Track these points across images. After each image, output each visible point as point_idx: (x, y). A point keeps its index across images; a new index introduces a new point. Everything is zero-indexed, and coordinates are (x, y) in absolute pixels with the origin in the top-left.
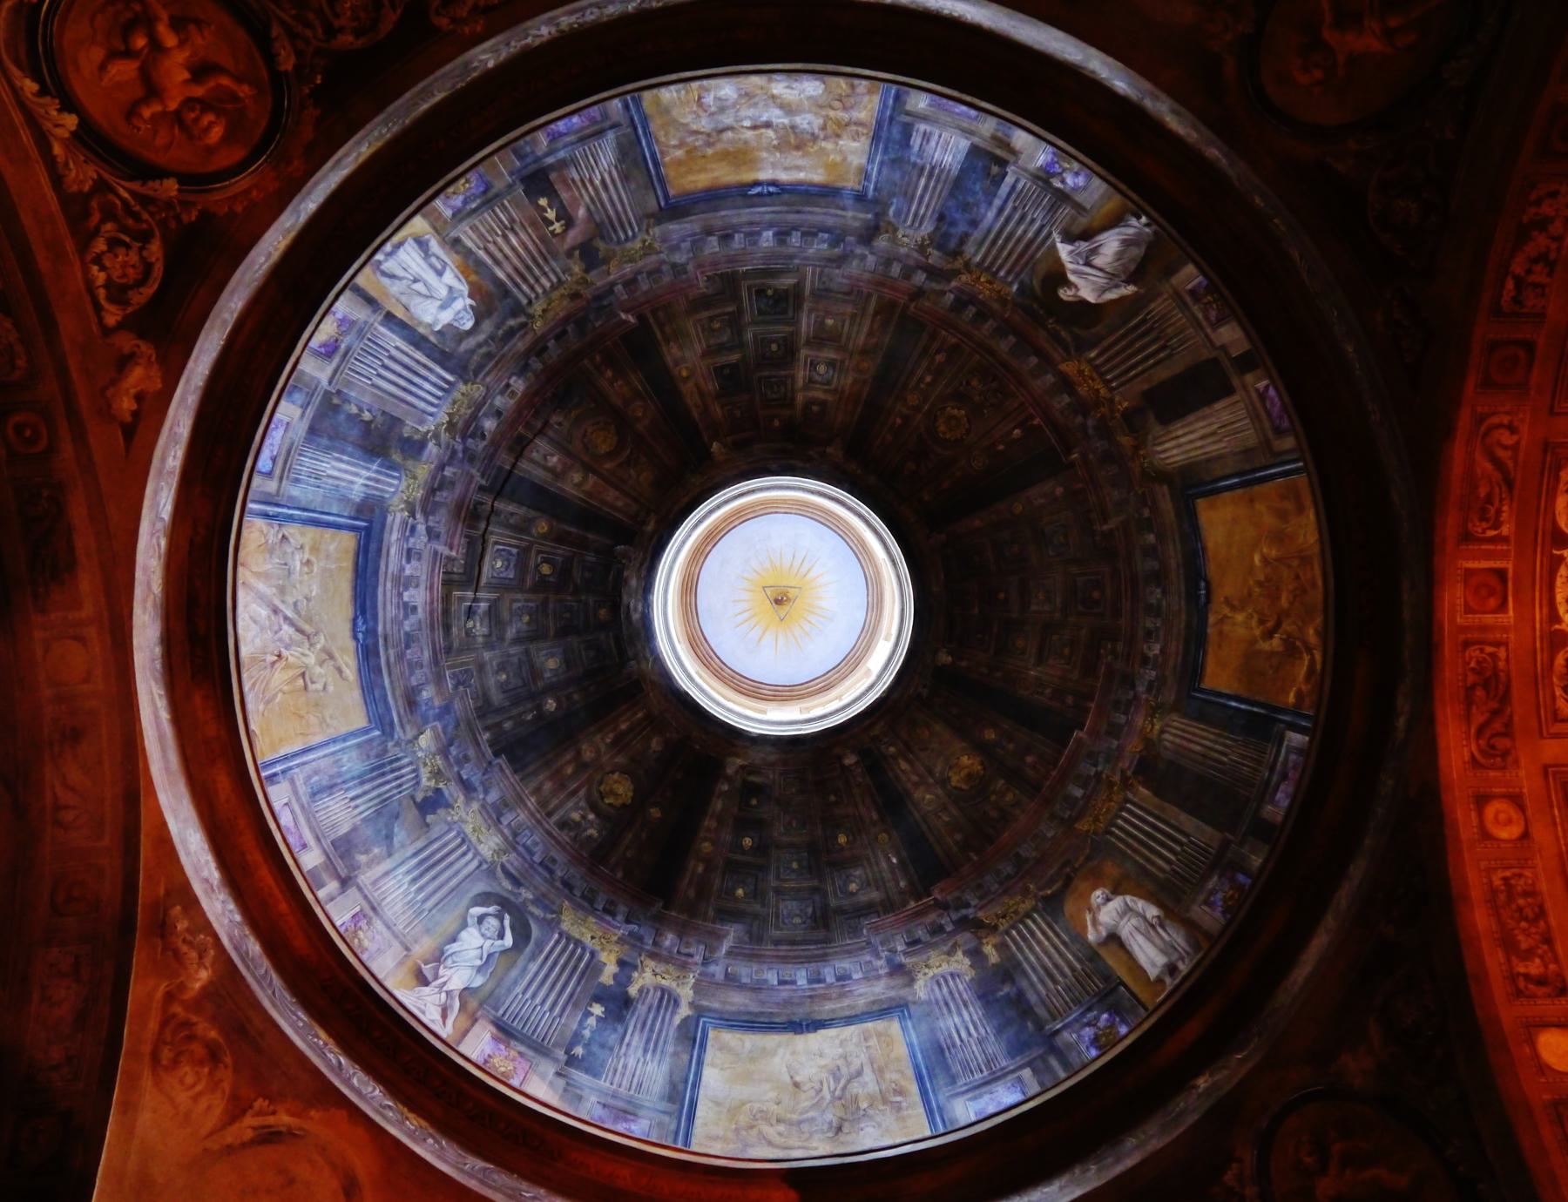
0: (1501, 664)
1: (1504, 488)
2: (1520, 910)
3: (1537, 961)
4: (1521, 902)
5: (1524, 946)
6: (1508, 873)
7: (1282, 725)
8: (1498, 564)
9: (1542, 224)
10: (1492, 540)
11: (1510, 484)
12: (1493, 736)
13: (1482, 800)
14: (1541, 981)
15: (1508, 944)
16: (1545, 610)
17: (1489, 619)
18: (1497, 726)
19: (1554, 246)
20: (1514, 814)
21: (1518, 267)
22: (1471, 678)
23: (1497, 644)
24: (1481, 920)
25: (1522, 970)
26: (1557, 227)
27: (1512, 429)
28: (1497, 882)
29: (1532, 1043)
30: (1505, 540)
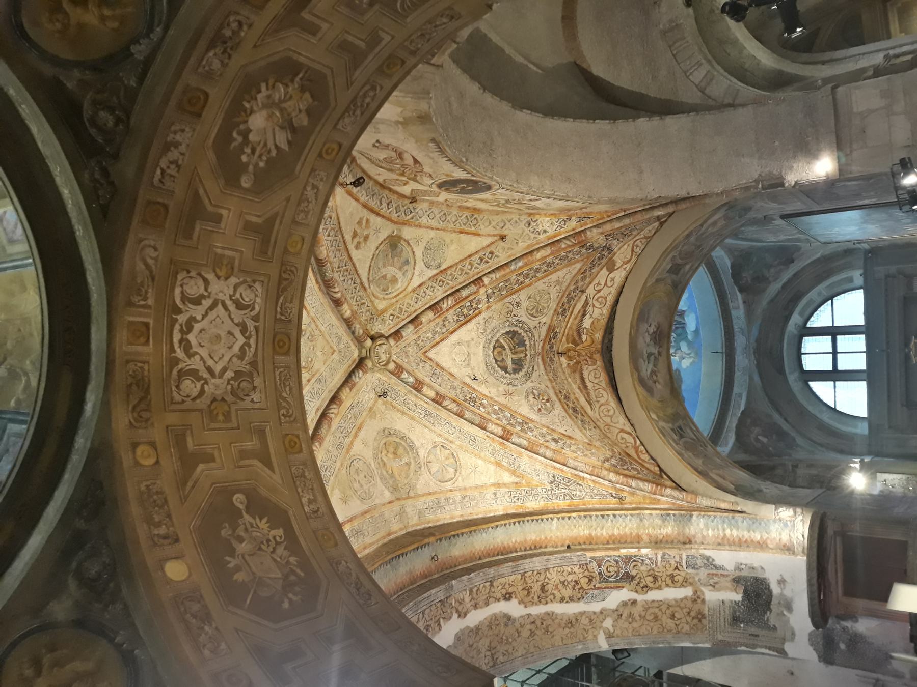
0: (146, 373)
1: (150, 279)
2: (155, 501)
3: (164, 526)
4: (155, 497)
5: (157, 520)
6: (148, 483)
7: (5, 421)
8: (145, 320)
9: (177, 145)
10: (143, 307)
11: (153, 279)
12: (141, 411)
13: (135, 446)
14: (165, 537)
15: (149, 521)
16: (168, 346)
17: (140, 348)
18: (143, 406)
19: (181, 157)
20: (152, 452)
21: (163, 163)
22: (130, 380)
23: (144, 363)
24: (135, 510)
25: (156, 532)
26: (183, 148)
27: (156, 249)
28: (143, 488)
29: (162, 569)
30: (149, 307)
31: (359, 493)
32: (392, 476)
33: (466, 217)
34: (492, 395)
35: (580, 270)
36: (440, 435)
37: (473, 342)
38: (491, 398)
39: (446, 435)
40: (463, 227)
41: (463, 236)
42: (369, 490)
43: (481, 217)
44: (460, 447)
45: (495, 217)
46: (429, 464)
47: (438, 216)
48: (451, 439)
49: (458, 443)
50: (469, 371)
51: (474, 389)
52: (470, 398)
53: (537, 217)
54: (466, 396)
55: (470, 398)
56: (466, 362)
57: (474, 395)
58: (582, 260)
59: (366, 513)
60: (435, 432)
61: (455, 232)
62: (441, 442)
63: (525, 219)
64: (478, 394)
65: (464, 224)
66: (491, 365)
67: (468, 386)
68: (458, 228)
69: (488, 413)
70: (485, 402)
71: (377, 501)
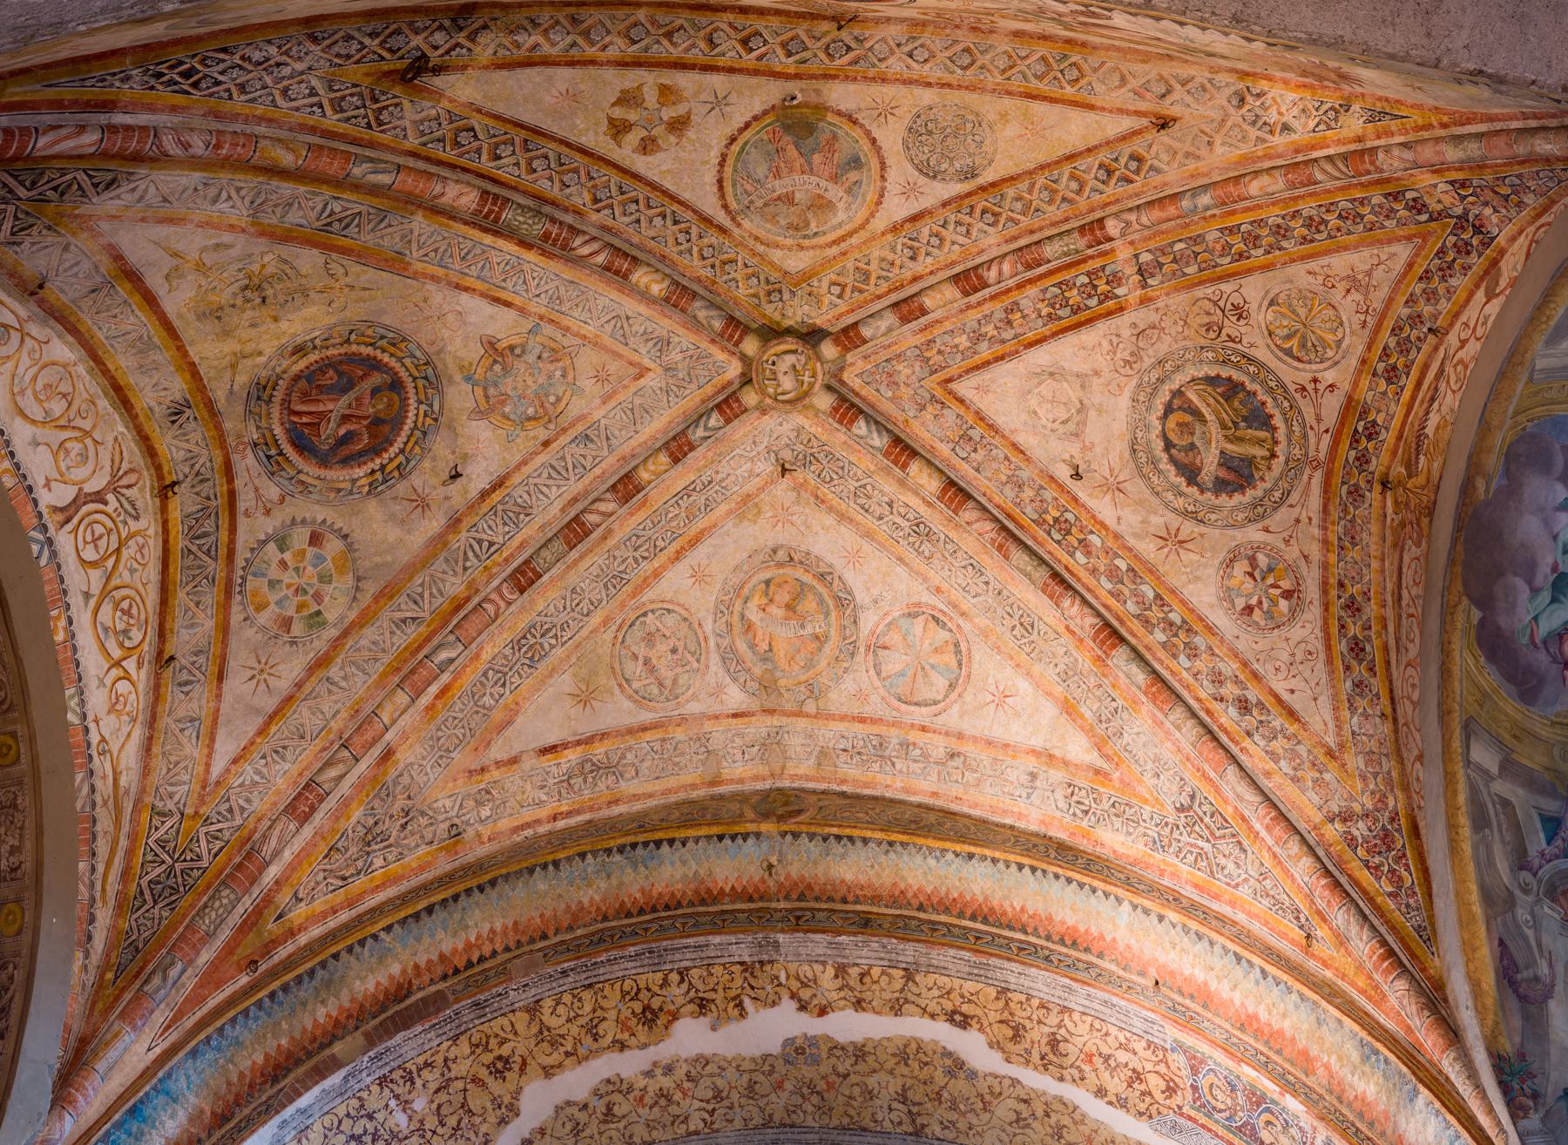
31: (635, 685)
32: (767, 656)
33: (1043, 58)
34: (1121, 529)
35: (1410, 265)
36: (938, 590)
37: (1096, 381)
38: (1117, 536)
39: (956, 595)
40: (1034, 83)
41: (1038, 107)
42: (675, 681)
43: (1094, 61)
44: (985, 634)
45: (1138, 67)
46: (881, 652)
47: (942, 56)
48: (965, 606)
49: (982, 621)
50: (1073, 449)
51: (1076, 500)
52: (1056, 520)
53: (1263, 85)
54: (1046, 512)
55: (1056, 520)
56: (1071, 426)
57: (1069, 516)
58: (1409, 238)
59: (644, 729)
60: (925, 579)
61: (1009, 93)
62: (934, 608)
63: (1232, 84)
64: (1084, 516)
65: (1040, 78)
66: (1149, 452)
67: (1061, 487)
68: (1016, 84)
69: (1094, 571)
70: (1094, 540)
71: (694, 708)
